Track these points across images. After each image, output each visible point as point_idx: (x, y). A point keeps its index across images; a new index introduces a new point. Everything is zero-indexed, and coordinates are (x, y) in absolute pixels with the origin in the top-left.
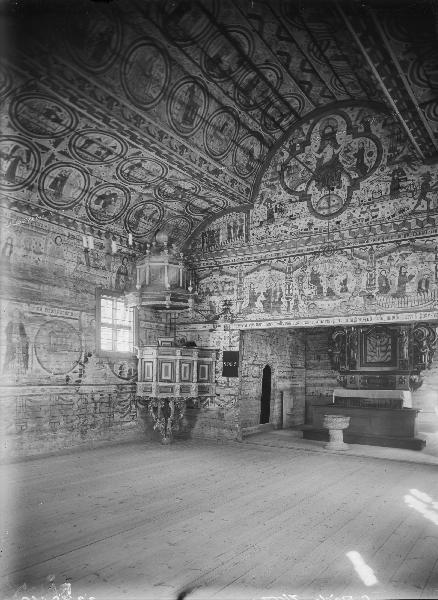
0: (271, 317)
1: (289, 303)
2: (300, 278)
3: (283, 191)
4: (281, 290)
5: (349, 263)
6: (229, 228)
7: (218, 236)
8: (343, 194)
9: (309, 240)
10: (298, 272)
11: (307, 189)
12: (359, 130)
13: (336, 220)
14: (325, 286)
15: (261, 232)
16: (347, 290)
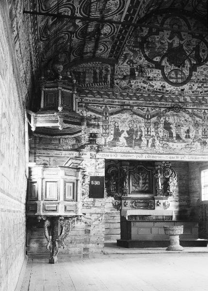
0: (133, 151)
1: (148, 141)
2: (156, 124)
3: (143, 58)
4: (142, 132)
5: (190, 119)
6: (95, 73)
7: (85, 77)
8: (186, 72)
9: (162, 97)
10: (154, 119)
11: (161, 61)
12: (196, 35)
13: (182, 88)
14: (174, 131)
15: (124, 83)
16: (189, 137)
